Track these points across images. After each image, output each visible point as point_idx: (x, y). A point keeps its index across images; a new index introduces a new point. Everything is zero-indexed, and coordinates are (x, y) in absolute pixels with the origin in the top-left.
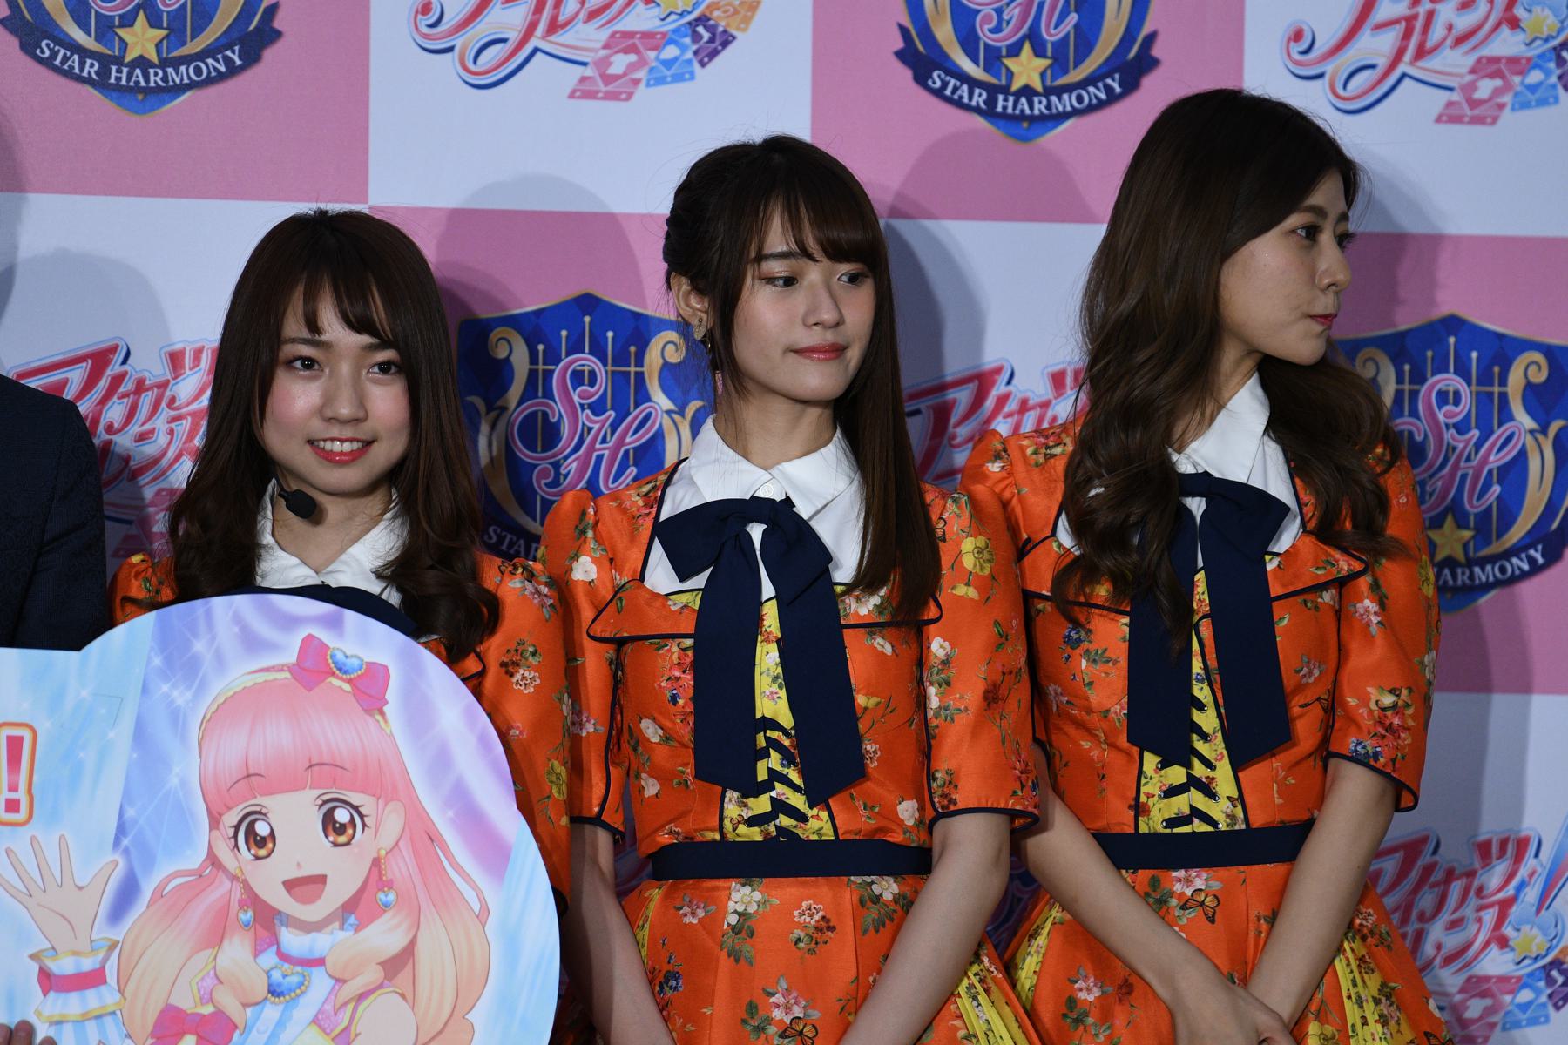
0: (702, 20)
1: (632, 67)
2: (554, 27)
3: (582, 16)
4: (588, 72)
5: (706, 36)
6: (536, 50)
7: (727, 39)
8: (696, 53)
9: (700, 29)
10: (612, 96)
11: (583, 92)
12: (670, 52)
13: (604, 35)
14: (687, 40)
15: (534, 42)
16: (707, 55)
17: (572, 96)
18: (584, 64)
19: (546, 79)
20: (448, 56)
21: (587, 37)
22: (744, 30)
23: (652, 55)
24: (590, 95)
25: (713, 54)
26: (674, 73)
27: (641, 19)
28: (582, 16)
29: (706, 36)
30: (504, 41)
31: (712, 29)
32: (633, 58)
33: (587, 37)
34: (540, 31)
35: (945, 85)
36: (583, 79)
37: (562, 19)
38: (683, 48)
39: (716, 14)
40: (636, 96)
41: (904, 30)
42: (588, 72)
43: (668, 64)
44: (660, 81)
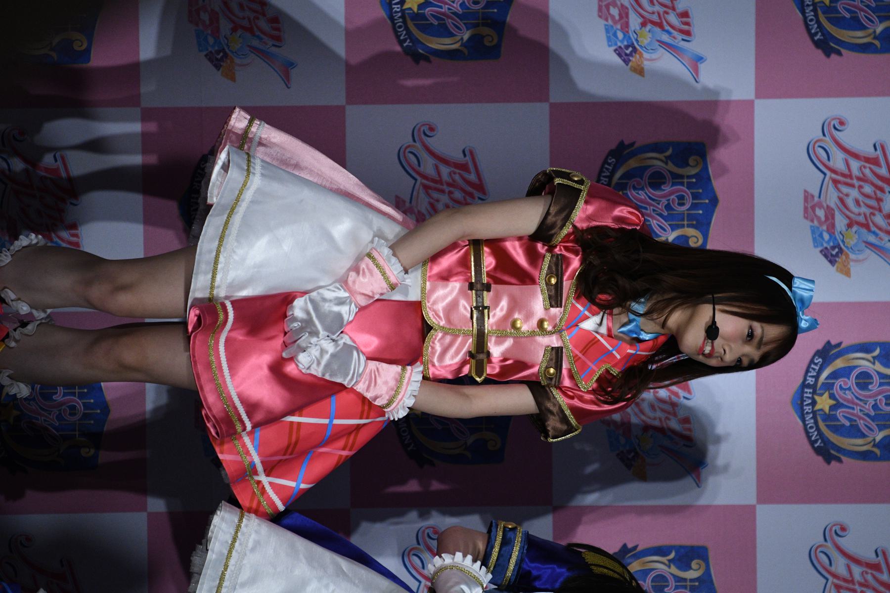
0: (841, 251)
1: (819, 218)
2: (835, 182)
3: (841, 195)
4: (816, 199)
5: (834, 253)
6: (825, 174)
7: (832, 262)
8: (826, 248)
9: (837, 250)
10: (806, 209)
11: (807, 197)
12: (826, 236)
13: (832, 205)
14: (832, 244)
15: (828, 173)
16: (825, 253)
17: (805, 191)
18: (820, 197)
19: (812, 179)
20: (821, 134)
21: (832, 198)
22: (837, 270)
23: (825, 228)
24: (806, 200)
25: (826, 256)
26: (817, 239)
27: (840, 222)
28: (841, 195)
29: (834, 253)
30: (829, 159)
31: (837, 255)
32: (823, 219)
33: (832, 198)
34: (834, 176)
35: (816, 364)
36: (813, 196)
37: (839, 186)
38: (828, 242)
39: (844, 257)
40: (805, 221)
41: (839, 344)
42: (816, 199)
43: (821, 235)
44: (813, 232)
